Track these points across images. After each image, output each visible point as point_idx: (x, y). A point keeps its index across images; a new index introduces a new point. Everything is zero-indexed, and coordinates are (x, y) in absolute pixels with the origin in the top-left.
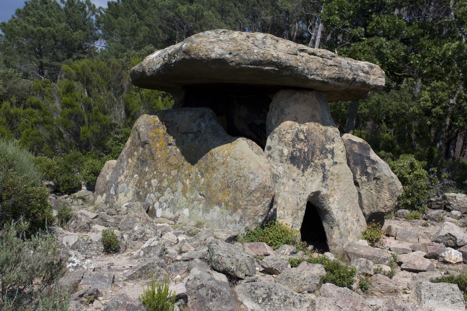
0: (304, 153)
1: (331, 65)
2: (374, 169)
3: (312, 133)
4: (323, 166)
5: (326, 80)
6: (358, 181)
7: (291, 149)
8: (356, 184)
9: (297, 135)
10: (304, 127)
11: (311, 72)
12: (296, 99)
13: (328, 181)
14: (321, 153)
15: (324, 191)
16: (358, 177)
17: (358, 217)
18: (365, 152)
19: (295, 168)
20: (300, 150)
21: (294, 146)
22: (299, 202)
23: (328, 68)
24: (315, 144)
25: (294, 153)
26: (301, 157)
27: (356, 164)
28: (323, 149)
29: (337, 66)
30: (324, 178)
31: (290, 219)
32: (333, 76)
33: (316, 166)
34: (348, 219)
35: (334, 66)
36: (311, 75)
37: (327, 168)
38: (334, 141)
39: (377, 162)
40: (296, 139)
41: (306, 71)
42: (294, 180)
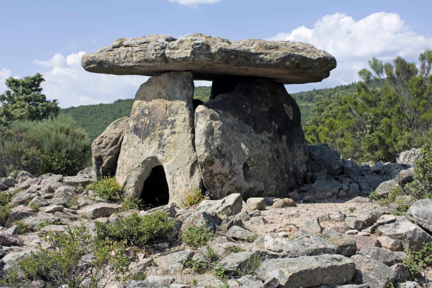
1: (137, 51)
3: (156, 108)
4: (161, 135)
5: (136, 64)
9: (142, 112)
10: (150, 104)
11: (121, 61)
15: (160, 157)
17: (187, 183)
20: (142, 123)
22: (134, 164)
29: (142, 51)
32: (140, 60)
34: (176, 182)
35: (140, 51)
36: (122, 63)
38: (177, 113)
41: (116, 61)
42: (135, 147)
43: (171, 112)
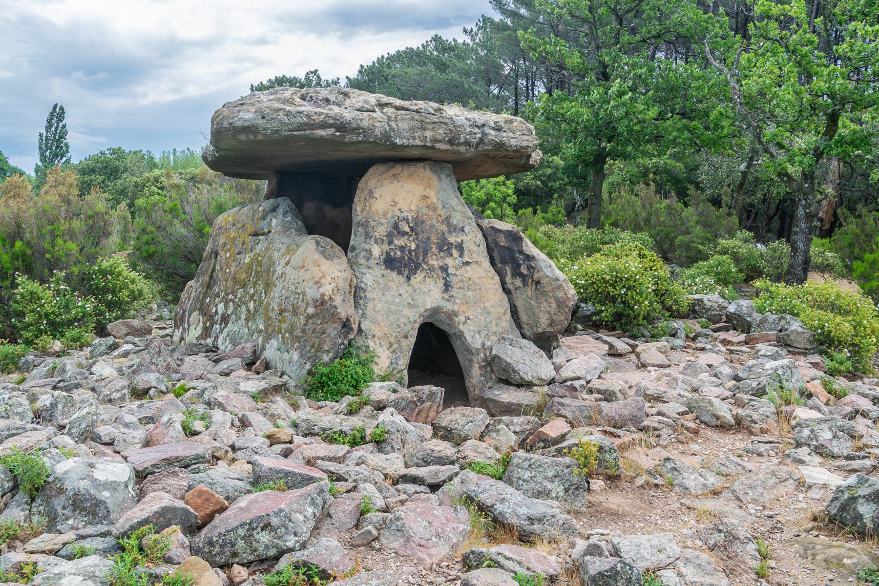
0: (410, 251)
1: (434, 123)
2: (530, 268)
3: (423, 222)
4: (444, 269)
6: (511, 287)
7: (386, 247)
8: (507, 291)
9: (396, 226)
12: (394, 175)
13: (454, 292)
14: (441, 250)
16: (508, 279)
18: (517, 244)
19: (394, 274)
20: (402, 249)
21: (391, 242)
23: (430, 126)
24: (429, 238)
25: (392, 254)
26: (404, 258)
27: (504, 262)
28: (444, 245)
30: (447, 286)
31: (388, 351)
33: (431, 269)
37: (450, 271)
38: (463, 231)
39: (533, 257)
40: (396, 230)
43: (453, 229)
